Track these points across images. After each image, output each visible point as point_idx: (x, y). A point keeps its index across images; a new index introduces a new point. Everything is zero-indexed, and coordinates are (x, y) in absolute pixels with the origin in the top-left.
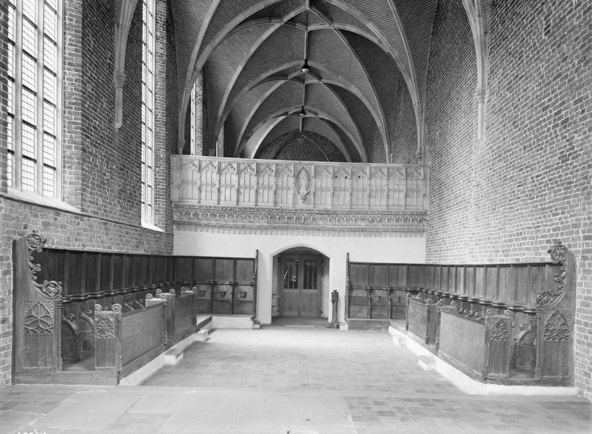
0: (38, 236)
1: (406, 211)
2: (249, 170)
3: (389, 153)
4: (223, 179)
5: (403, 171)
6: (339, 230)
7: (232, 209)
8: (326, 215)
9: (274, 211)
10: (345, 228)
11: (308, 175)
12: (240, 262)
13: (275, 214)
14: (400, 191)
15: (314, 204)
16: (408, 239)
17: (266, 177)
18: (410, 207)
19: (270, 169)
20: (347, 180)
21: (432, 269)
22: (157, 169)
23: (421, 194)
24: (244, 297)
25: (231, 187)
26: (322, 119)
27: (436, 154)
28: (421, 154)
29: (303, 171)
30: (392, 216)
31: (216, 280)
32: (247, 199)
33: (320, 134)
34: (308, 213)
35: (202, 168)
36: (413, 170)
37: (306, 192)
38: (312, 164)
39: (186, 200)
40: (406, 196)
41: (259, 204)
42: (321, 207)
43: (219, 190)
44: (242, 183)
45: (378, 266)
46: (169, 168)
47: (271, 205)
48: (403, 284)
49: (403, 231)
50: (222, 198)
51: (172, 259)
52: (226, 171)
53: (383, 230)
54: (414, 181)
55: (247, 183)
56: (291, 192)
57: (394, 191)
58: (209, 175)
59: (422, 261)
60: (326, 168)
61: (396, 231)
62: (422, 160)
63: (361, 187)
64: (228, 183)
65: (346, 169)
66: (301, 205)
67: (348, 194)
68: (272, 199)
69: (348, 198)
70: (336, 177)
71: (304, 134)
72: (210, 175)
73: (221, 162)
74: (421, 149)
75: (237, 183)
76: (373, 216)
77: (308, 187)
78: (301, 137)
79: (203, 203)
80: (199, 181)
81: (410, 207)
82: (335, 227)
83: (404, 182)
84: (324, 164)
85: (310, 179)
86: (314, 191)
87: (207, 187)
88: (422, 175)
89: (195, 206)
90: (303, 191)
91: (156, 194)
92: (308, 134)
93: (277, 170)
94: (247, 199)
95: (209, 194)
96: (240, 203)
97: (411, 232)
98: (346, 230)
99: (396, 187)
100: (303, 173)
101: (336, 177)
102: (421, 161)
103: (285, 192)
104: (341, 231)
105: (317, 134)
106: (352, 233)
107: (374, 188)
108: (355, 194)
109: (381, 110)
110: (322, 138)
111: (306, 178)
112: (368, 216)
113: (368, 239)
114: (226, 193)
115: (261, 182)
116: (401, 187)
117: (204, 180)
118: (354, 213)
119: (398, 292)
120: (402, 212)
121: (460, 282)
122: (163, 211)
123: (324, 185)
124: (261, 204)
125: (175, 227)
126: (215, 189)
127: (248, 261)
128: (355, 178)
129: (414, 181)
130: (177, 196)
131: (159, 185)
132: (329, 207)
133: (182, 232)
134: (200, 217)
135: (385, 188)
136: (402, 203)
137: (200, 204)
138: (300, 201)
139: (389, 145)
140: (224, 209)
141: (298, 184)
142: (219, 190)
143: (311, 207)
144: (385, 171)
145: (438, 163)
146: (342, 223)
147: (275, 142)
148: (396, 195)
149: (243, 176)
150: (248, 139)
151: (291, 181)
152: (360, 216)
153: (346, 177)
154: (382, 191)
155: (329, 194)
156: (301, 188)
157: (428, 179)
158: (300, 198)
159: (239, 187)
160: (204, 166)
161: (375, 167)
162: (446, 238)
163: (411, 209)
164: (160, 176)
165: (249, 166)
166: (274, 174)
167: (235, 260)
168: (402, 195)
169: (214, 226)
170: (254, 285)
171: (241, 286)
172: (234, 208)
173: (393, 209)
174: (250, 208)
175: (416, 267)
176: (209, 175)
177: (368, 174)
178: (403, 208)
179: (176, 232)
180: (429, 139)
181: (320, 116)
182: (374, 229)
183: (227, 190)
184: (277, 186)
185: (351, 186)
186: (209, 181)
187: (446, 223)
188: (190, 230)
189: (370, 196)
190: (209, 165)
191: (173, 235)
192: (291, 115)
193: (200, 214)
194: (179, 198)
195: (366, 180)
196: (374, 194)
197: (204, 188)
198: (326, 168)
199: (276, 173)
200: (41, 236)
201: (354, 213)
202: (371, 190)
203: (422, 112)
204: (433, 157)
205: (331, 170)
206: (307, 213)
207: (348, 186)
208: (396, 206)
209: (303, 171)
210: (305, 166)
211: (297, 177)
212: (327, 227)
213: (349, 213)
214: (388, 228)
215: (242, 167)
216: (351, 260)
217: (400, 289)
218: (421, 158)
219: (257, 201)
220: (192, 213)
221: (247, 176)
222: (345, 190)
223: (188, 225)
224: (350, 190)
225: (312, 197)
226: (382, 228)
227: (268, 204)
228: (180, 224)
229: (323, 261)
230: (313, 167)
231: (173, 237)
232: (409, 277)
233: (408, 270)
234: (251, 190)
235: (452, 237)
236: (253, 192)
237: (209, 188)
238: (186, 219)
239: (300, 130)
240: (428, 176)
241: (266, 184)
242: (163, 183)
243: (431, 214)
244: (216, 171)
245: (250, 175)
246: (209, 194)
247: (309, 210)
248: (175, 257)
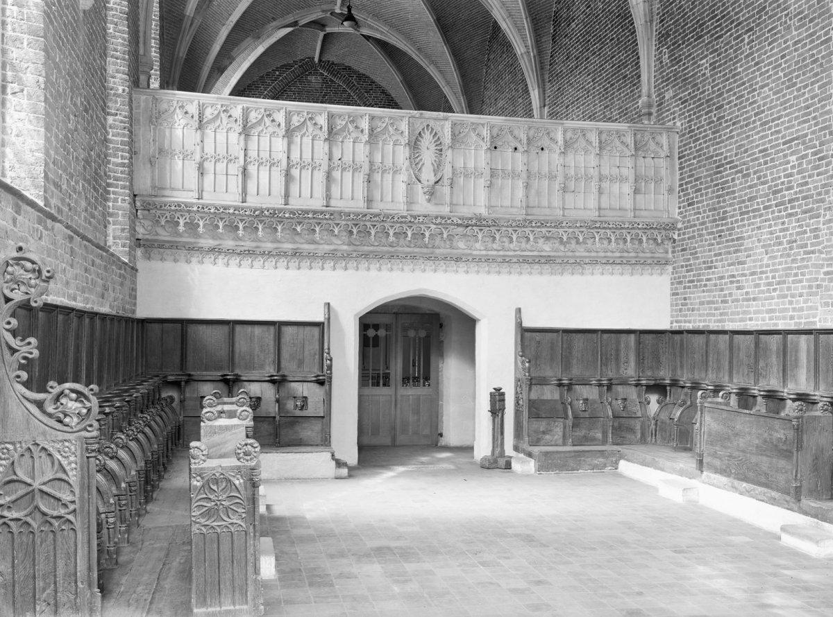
0: (33, 262)
1: (637, 220)
2: (311, 129)
3: (540, 107)
4: (253, 145)
5: (629, 139)
6: (500, 259)
7: (274, 213)
8: (474, 228)
9: (368, 218)
10: (511, 256)
11: (438, 143)
13: (368, 224)
14: (622, 179)
15: (451, 204)
16: (636, 278)
17: (349, 144)
18: (643, 213)
19: (357, 127)
21: (700, 339)
23: (664, 186)
24: (302, 408)
25: (272, 165)
26: (367, 38)
27: (702, 104)
28: (650, 106)
29: (428, 133)
30: (608, 231)
31: (237, 371)
32: (306, 192)
33: (356, 68)
34: (440, 224)
35: (205, 121)
36: (647, 136)
37: (433, 179)
38: (446, 119)
39: (167, 193)
40: (637, 191)
41: (333, 203)
42: (465, 211)
43: (245, 171)
44: (295, 156)
45: (580, 335)
47: (359, 205)
48: (630, 371)
49: (628, 263)
52: (260, 128)
53: (587, 260)
54: (649, 160)
55: (307, 156)
56: (403, 177)
57: (612, 179)
58: (221, 137)
59: (665, 326)
60: (474, 127)
61: (613, 263)
62: (652, 117)
63: (546, 169)
64: (265, 155)
65: (516, 132)
66: (423, 206)
67: (520, 184)
68: (360, 193)
69: (520, 193)
70: (495, 148)
71: (323, 67)
72: (225, 138)
73: (248, 108)
74: (649, 96)
75: (286, 155)
76: (571, 230)
77: (438, 167)
78: (316, 74)
79: (208, 199)
80: (198, 148)
81: (643, 213)
82: (490, 253)
83: (629, 162)
84: (472, 120)
85: (441, 150)
86: (450, 175)
87: (217, 164)
88: (665, 147)
89: (192, 205)
90: (428, 176)
92: (331, 67)
93: (372, 130)
94: (306, 192)
95: (221, 179)
96: (291, 201)
97: (643, 264)
98: (515, 260)
99: (615, 171)
100: (427, 140)
101: (495, 148)
102: (649, 120)
103: (389, 177)
104: (504, 261)
105: (350, 68)
106: (527, 266)
107: (573, 173)
108: (535, 184)
109: (526, 18)
110: (361, 77)
111: (433, 147)
112: (561, 231)
113: (557, 278)
114: (260, 177)
115: (337, 154)
116: (625, 172)
117: (209, 149)
118: (534, 225)
119: (620, 388)
120: (630, 223)
121: (796, 365)
122: (123, 216)
123: (471, 165)
124: (337, 204)
126: (235, 169)
127: (308, 329)
128: (534, 151)
129: (649, 160)
130: (149, 182)
132: (483, 211)
133: (156, 264)
134: (201, 230)
135: (593, 173)
136: (628, 203)
137: (200, 201)
138: (421, 198)
139: (541, 89)
140: (257, 213)
141: (417, 160)
142: (245, 171)
144: (594, 138)
145: (709, 124)
146: (506, 244)
147: (263, 83)
148: (616, 187)
149: (297, 140)
150: (222, 72)
152: (544, 230)
153: (516, 149)
154: (588, 178)
155: (482, 182)
156: (424, 169)
157: (677, 156)
158: (421, 191)
159: (288, 164)
160: (211, 117)
161: (574, 130)
162: (744, 275)
163: (646, 217)
165: (311, 119)
166: (365, 137)
167: (279, 325)
168: (627, 188)
169: (231, 252)
170: (323, 382)
171: (293, 384)
172: (280, 210)
173: (611, 216)
174: (315, 212)
175: (654, 336)
176: (221, 137)
177: (561, 142)
178: (630, 215)
179: (141, 265)
180: (674, 75)
181: (365, 31)
182: (572, 257)
183: (261, 173)
184: (371, 163)
185: (525, 168)
186: (222, 150)
187: (742, 245)
188: (176, 261)
189: (565, 190)
190: (222, 114)
192: (303, 26)
193: (201, 223)
194: (154, 187)
195: (556, 156)
196: (572, 185)
197: (209, 166)
198: (474, 130)
199: (370, 135)
200: (39, 262)
201: (534, 225)
202: (566, 177)
203: (651, 21)
204: (688, 111)
205: (485, 132)
206: (436, 224)
207: (520, 167)
208: (615, 209)
209: (428, 133)
210: (432, 123)
211: (414, 145)
212: (475, 253)
213: (526, 223)
214: (597, 257)
215: (296, 120)
216: (527, 323)
217: (624, 383)
218: (650, 114)
219: (328, 197)
220: (182, 222)
221: (307, 140)
222: (514, 175)
223: (171, 247)
224: (524, 175)
225: (447, 190)
226: (586, 257)
227: (352, 204)
229: (441, 326)
230: (448, 125)
232: (641, 357)
233: (639, 343)
234: (316, 172)
235: (762, 273)
236: (320, 176)
237: (221, 167)
238: (164, 235)
239: (316, 60)
240: (677, 151)
241: (348, 158)
243: (686, 228)
244: (239, 129)
245: (313, 140)
246: (221, 179)
247: (442, 218)
248: (144, 322)
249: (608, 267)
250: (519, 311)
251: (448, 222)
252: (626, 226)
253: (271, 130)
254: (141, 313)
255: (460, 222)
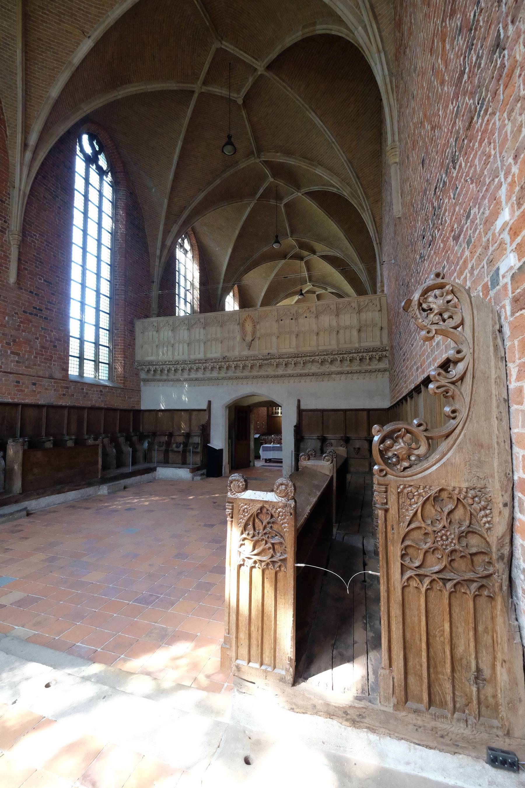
12: (195, 413)
20: (293, 321)
22: (116, 331)
37: (251, 338)
46: (132, 332)
50: (176, 354)
51: (119, 412)
55: (197, 337)
66: (246, 353)
77: (254, 333)
85: (255, 325)
90: (249, 338)
91: (115, 354)
111: (251, 325)
125: (142, 383)
131: (118, 345)
132: (274, 351)
143: (256, 352)
151: (237, 328)
164: (119, 337)
174: (199, 360)
186: (166, 339)
191: (140, 391)
216: (303, 407)
228: (145, 381)
231: (140, 394)
242: (120, 343)
249: (350, 375)
250: (299, 401)
251: (257, 358)
252: (354, 351)
253: (184, 328)
254: (143, 408)
255: (263, 358)
